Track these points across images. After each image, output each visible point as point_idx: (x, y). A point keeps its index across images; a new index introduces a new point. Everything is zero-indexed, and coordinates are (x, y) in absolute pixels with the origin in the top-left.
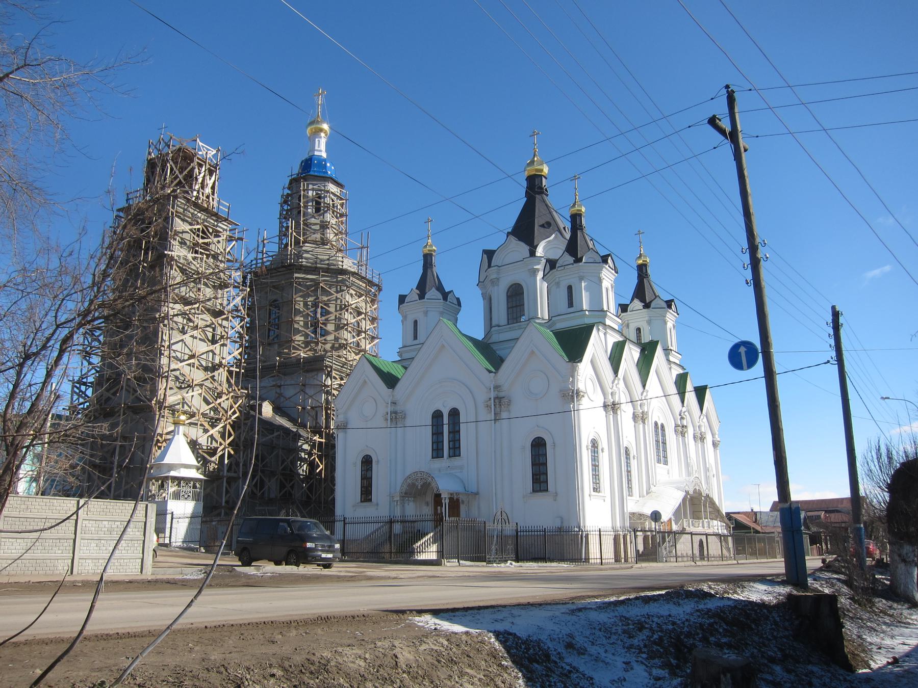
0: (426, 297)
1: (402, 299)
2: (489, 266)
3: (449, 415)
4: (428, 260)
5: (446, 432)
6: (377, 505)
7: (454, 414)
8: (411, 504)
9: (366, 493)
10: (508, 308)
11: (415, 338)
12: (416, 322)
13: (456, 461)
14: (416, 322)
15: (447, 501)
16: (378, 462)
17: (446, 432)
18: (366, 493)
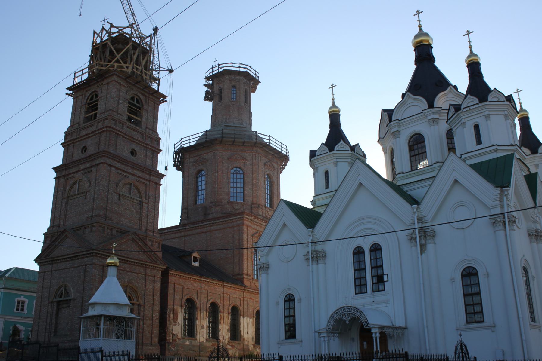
0: (336, 148)
1: (313, 154)
2: (390, 121)
3: (371, 251)
4: (335, 118)
5: (369, 269)
6: (302, 342)
7: (376, 249)
8: (337, 340)
9: (290, 332)
10: (411, 157)
11: (327, 186)
12: (327, 173)
13: (380, 296)
14: (327, 173)
15: (378, 335)
16: (300, 300)
17: (369, 269)
18: (290, 332)
